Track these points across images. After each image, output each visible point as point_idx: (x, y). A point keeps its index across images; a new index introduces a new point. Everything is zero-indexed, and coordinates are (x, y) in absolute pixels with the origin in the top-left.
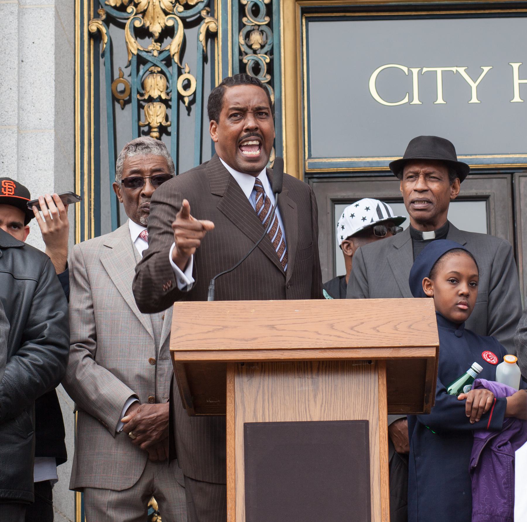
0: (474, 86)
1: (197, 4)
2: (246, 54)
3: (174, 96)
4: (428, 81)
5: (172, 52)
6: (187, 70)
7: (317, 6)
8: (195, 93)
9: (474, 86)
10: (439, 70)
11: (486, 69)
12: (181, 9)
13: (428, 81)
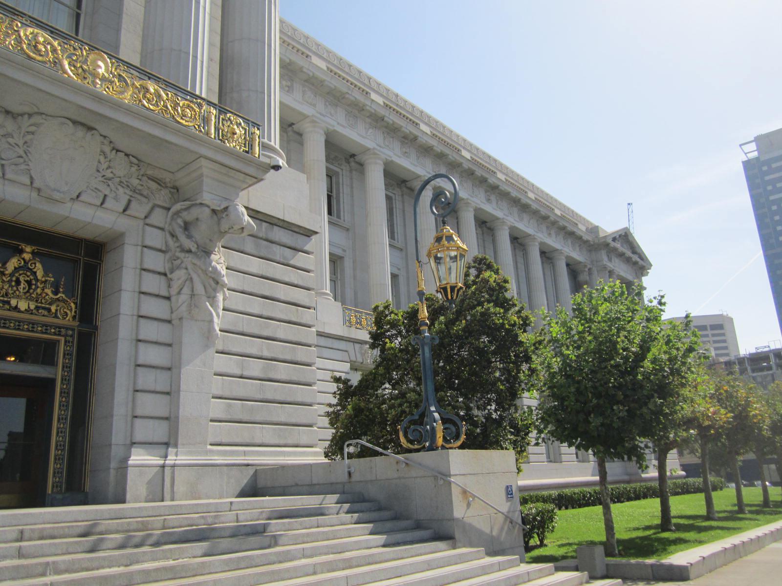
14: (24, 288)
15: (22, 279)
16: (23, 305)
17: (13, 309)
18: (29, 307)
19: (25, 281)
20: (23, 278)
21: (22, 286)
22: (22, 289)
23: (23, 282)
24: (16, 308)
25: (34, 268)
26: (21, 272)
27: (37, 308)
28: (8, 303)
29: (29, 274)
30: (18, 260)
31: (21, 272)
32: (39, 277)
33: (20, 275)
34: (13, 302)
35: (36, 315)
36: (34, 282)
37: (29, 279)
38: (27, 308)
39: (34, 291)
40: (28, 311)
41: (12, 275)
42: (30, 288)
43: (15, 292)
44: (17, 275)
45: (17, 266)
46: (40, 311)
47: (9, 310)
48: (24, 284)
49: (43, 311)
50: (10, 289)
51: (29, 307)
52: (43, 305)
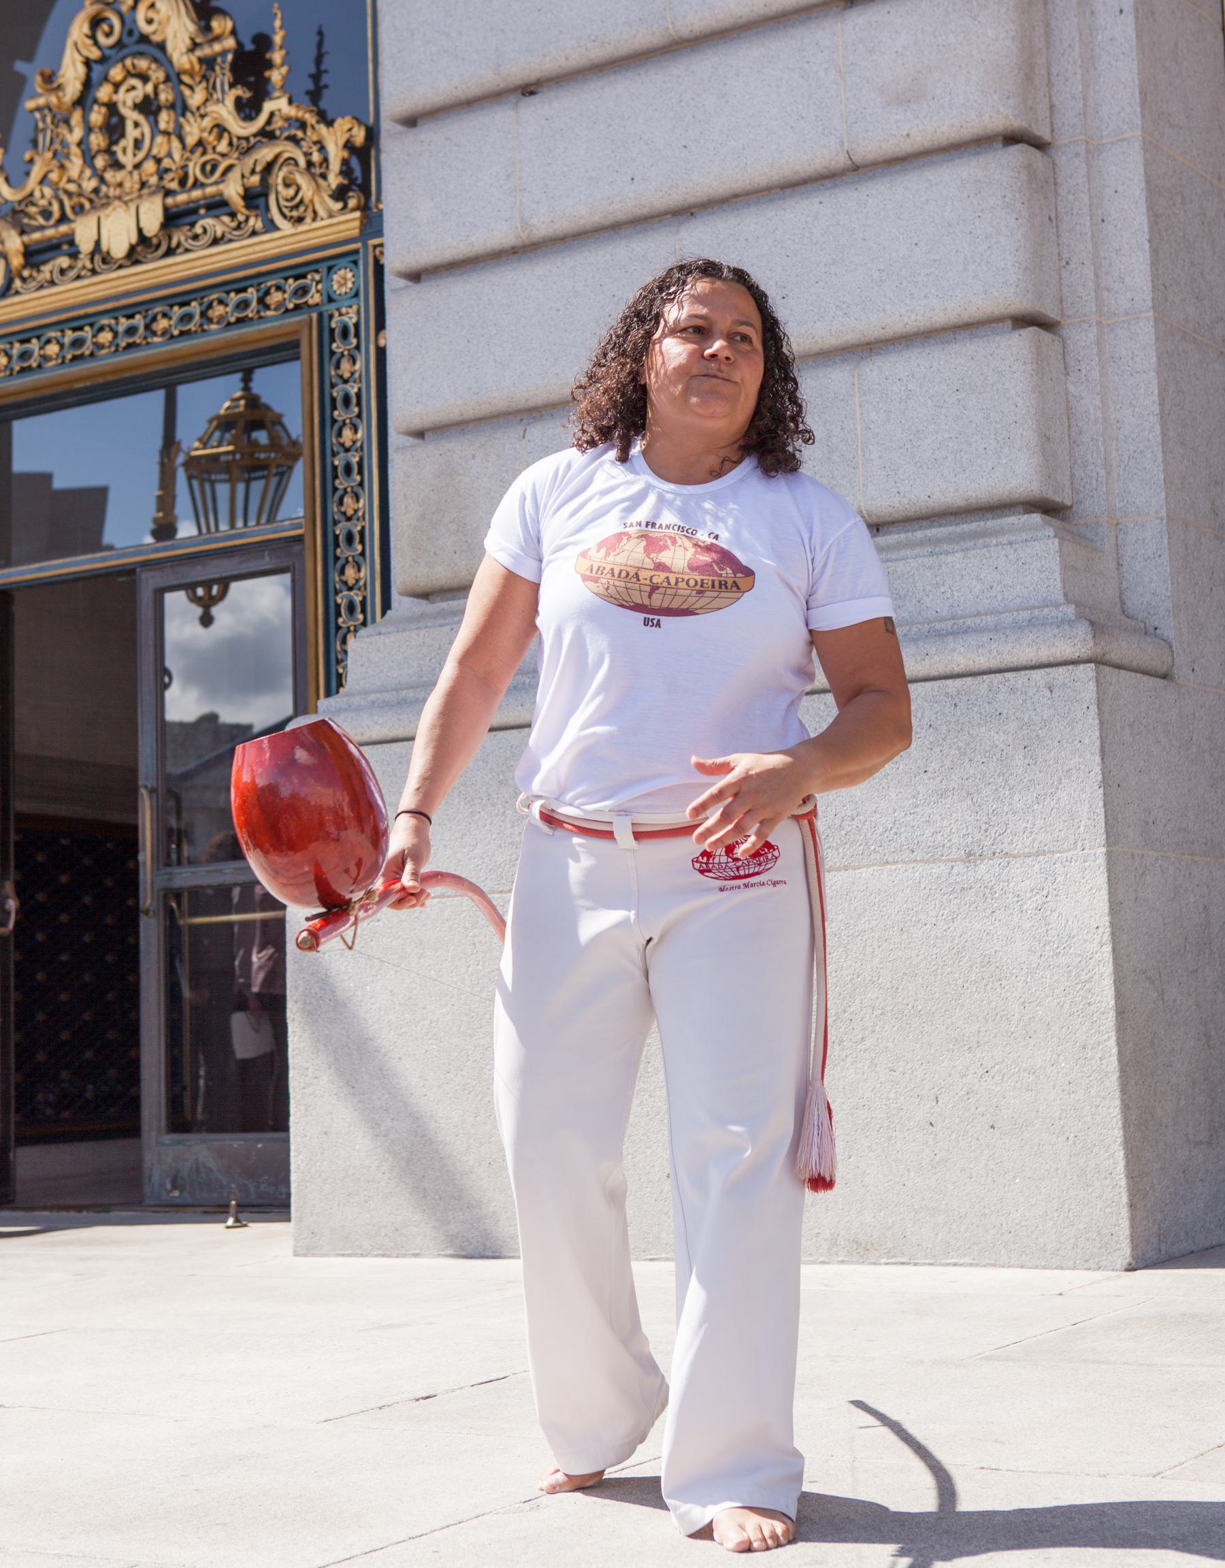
15: (127, 99)
18: (140, 231)
21: (131, 133)
22: (130, 151)
23: (131, 116)
29: (143, 64)
31: (116, 73)
33: (117, 86)
34: (84, 232)
35: (187, 250)
36: (165, 96)
40: (142, 247)
41: (84, 100)
45: (95, 54)
46: (198, 229)
48: (136, 125)
49: (208, 222)
51: (140, 231)
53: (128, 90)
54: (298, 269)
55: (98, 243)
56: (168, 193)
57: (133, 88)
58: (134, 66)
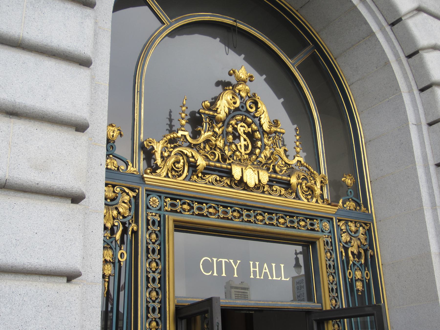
0: (235, 268)
1: (128, 216)
2: (149, 244)
3: (117, 261)
4: (219, 264)
5: (117, 239)
6: (122, 248)
7: (184, 225)
8: (126, 260)
9: (235, 268)
10: (223, 260)
11: (239, 261)
12: (121, 218)
13: (219, 264)
14: (246, 147)
15: (241, 130)
16: (251, 177)
17: (236, 184)
18: (259, 181)
19: (245, 133)
20: (242, 129)
21: (243, 143)
24: (242, 184)
25: (256, 111)
26: (238, 118)
27: (271, 180)
28: (229, 173)
29: (249, 120)
30: (233, 97)
31: (238, 118)
32: (266, 127)
34: (237, 172)
36: (258, 135)
37: (250, 130)
38: (257, 183)
39: (261, 153)
42: (254, 147)
43: (234, 152)
44: (233, 122)
47: (231, 187)
48: (245, 140)
50: (226, 148)
51: (259, 181)
52: (279, 177)
53: (241, 126)
54: (311, 217)
55: (242, 178)
56: (275, 172)
57: (244, 127)
58: (246, 118)
